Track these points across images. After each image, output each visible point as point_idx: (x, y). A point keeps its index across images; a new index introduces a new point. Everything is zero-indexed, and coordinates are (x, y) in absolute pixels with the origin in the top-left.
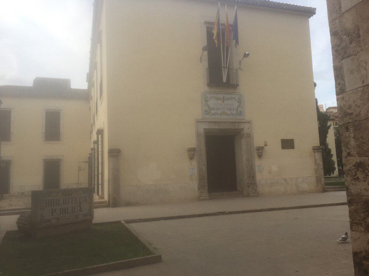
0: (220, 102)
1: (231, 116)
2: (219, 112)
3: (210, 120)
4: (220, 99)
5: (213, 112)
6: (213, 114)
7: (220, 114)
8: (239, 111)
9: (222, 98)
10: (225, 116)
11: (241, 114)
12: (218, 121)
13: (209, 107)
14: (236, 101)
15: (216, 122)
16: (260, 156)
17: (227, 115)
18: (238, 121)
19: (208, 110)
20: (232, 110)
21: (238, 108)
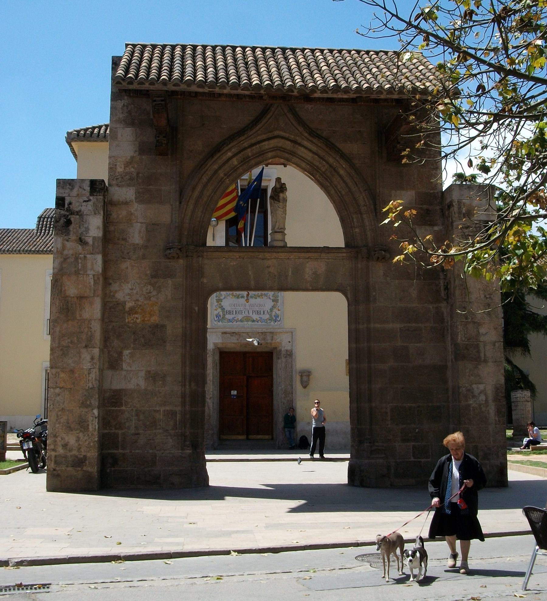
0: (242, 301)
1: (260, 323)
2: (240, 317)
3: (225, 330)
4: (243, 297)
5: (228, 317)
6: (229, 321)
7: (241, 321)
8: (273, 314)
9: (245, 295)
10: (250, 323)
11: (276, 319)
12: (237, 330)
13: (223, 309)
14: (270, 298)
15: (233, 333)
16: (305, 385)
17: (253, 321)
18: (272, 330)
19: (221, 313)
20: (262, 313)
21: (271, 310)
